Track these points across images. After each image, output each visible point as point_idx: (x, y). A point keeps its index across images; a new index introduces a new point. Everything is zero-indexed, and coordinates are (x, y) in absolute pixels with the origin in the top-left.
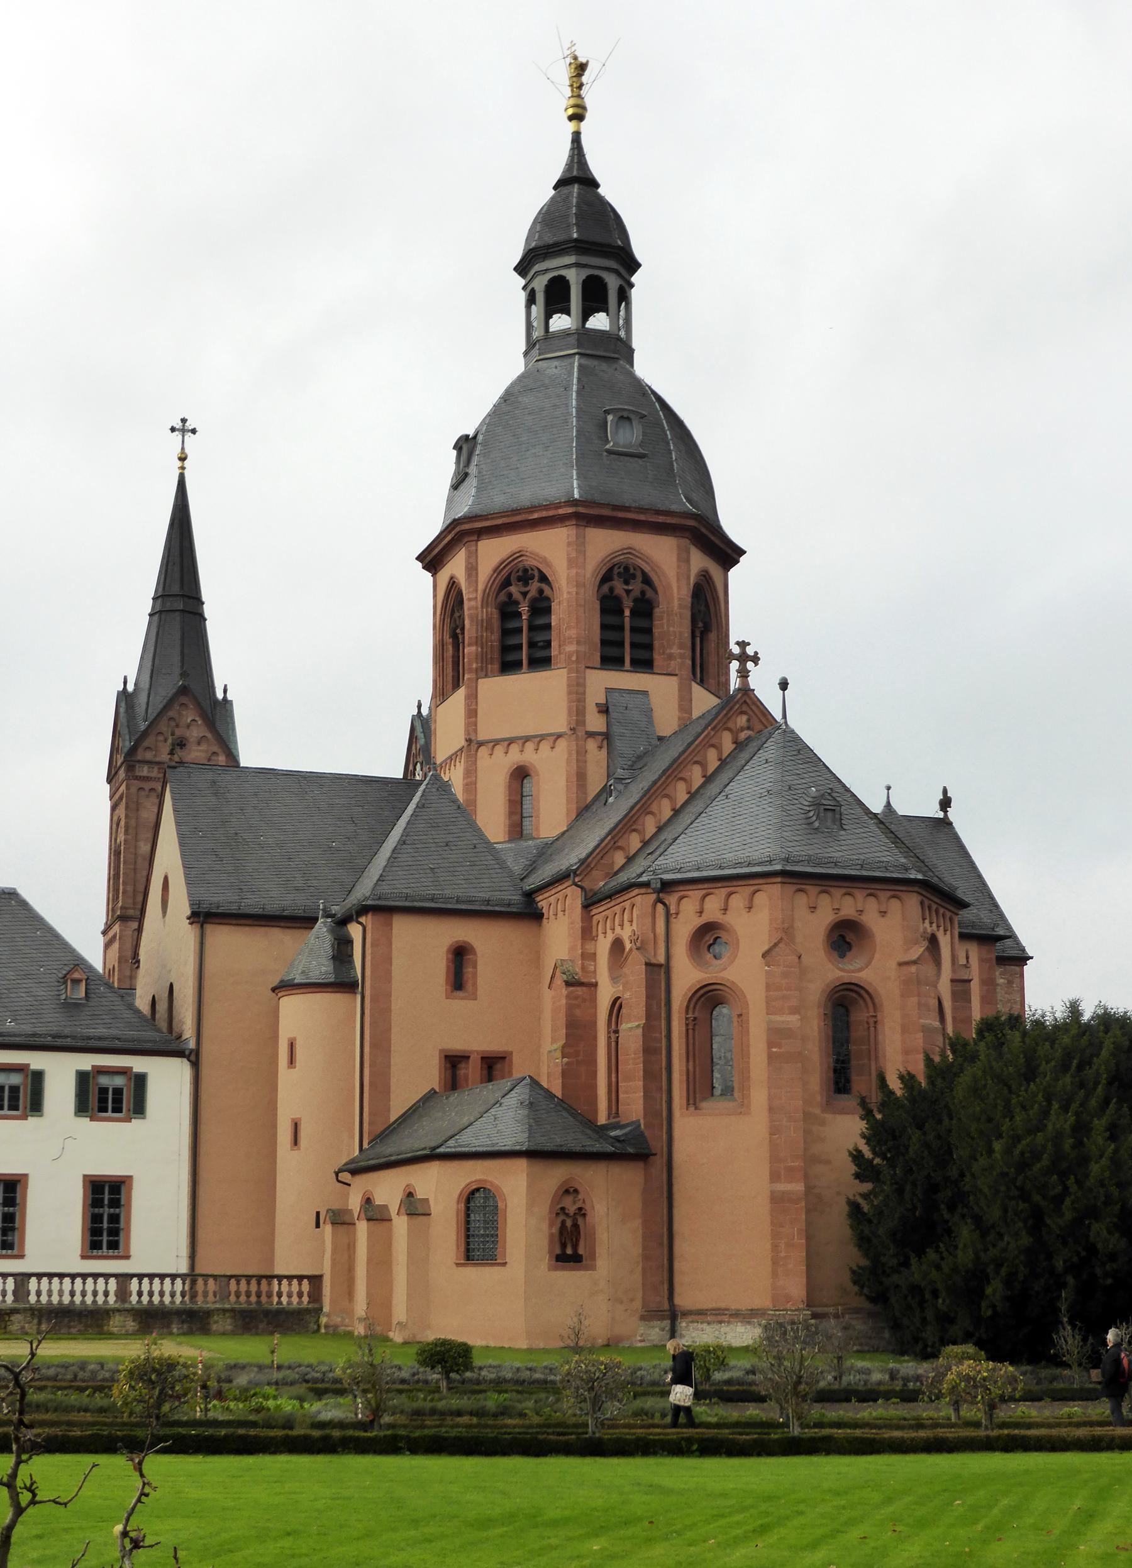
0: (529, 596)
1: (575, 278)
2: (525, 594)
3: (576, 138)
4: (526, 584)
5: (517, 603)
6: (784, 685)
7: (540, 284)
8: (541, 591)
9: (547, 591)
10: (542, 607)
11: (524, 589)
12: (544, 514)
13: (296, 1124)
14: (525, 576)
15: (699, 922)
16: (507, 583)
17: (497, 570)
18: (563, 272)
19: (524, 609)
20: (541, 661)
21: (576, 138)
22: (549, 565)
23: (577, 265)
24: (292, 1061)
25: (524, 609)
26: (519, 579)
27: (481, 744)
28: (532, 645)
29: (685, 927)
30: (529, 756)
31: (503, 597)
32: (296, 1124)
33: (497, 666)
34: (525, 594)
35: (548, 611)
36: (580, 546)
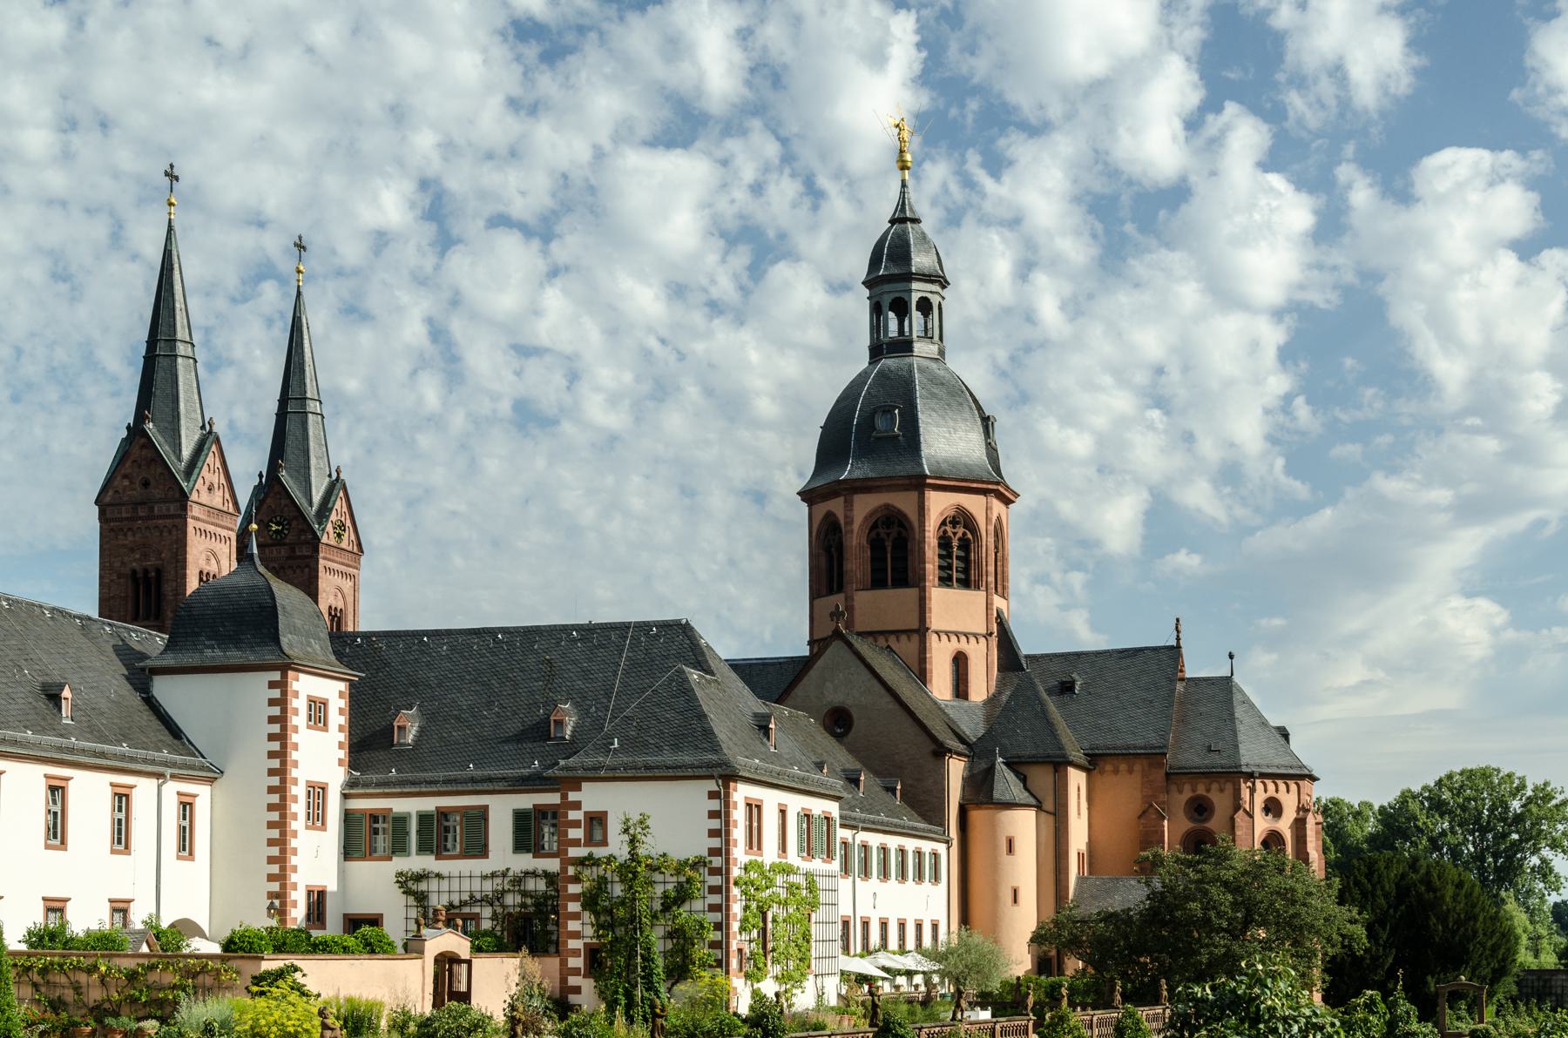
0: (957, 537)
2: (955, 534)
3: (904, 185)
4: (954, 528)
6: (1231, 656)
10: (965, 545)
12: (980, 486)
13: (1015, 890)
14: (954, 522)
16: (944, 523)
17: (941, 514)
18: (929, 296)
19: (955, 543)
20: (966, 583)
24: (1010, 850)
25: (955, 543)
26: (950, 522)
27: (937, 633)
28: (950, 567)
30: (963, 645)
32: (1015, 890)
33: (937, 579)
36: (988, 509)
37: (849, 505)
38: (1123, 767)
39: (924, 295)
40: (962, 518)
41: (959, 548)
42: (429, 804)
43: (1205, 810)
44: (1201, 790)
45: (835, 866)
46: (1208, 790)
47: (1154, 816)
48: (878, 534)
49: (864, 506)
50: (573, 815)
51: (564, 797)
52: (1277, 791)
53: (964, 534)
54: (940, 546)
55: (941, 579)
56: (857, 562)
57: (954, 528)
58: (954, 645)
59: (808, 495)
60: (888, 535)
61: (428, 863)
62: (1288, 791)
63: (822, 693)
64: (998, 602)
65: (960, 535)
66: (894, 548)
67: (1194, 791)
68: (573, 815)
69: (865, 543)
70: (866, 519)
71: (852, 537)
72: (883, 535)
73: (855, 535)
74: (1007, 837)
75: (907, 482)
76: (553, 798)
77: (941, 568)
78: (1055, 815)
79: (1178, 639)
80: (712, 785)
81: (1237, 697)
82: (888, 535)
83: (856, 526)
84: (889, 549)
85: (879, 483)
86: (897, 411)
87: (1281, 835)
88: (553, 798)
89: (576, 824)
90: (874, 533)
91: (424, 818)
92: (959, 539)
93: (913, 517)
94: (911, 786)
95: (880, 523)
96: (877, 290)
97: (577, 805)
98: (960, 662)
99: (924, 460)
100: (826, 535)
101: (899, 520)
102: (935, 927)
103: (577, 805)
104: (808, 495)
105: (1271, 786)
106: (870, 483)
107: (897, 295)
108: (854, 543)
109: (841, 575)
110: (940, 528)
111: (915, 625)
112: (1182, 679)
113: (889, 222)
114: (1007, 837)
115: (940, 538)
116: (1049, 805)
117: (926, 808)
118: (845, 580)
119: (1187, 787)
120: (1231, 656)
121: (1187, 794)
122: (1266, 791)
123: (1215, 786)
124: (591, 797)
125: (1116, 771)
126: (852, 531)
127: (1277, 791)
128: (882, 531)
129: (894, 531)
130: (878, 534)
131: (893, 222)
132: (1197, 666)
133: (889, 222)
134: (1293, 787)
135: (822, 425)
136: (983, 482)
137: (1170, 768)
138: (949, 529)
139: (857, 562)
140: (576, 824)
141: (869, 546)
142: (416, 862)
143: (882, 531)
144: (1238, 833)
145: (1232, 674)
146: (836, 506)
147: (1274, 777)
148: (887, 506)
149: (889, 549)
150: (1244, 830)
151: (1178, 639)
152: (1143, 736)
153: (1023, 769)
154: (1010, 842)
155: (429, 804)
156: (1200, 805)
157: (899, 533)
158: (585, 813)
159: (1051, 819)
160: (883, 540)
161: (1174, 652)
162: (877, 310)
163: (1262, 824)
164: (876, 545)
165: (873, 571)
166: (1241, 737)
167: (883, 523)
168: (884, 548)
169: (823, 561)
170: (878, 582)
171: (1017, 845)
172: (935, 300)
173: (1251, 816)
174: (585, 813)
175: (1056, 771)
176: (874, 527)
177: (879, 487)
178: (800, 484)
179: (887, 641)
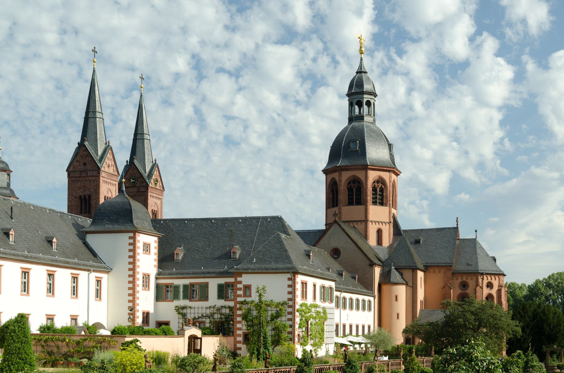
0: (379, 187)
2: (378, 186)
3: (361, 59)
4: (378, 184)
5: (376, 187)
6: (476, 231)
10: (382, 190)
11: (378, 185)
12: (387, 169)
13: (398, 314)
14: (378, 182)
15: (487, 281)
16: (374, 182)
17: (373, 179)
19: (378, 189)
21: (361, 59)
24: (396, 300)
25: (378, 189)
26: (376, 182)
27: (371, 222)
28: (376, 198)
29: (485, 282)
30: (381, 226)
32: (398, 314)
33: (371, 202)
37: (340, 175)
38: (437, 270)
39: (368, 99)
40: (381, 181)
41: (380, 191)
42: (187, 282)
43: (466, 286)
44: (464, 279)
45: (333, 305)
46: (467, 279)
47: (447, 288)
48: (350, 186)
49: (346, 176)
50: (239, 286)
51: (236, 279)
52: (491, 279)
53: (381, 186)
54: (373, 190)
55: (373, 202)
56: (343, 196)
57: (378, 184)
58: (377, 226)
59: (325, 171)
60: (354, 186)
61: (186, 303)
62: (495, 280)
63: (330, 243)
64: (393, 211)
65: (380, 186)
66: (356, 191)
67: (462, 279)
68: (239, 286)
69: (346, 189)
70: (346, 180)
71: (341, 187)
72: (352, 186)
73: (342, 186)
74: (395, 295)
75: (361, 167)
76: (231, 280)
77: (373, 198)
78: (412, 287)
79: (457, 225)
80: (289, 276)
81: (478, 246)
82: (354, 186)
83: (343, 183)
84: (354, 191)
85: (351, 168)
86: (358, 142)
87: (492, 295)
88: (231, 280)
89: (240, 289)
90: (349, 186)
91: (185, 287)
92: (380, 188)
93: (363, 179)
94: (361, 276)
95: (351, 181)
96: (352, 97)
97: (240, 282)
98: (379, 232)
99: (367, 160)
100: (332, 186)
101: (358, 181)
102: (369, 327)
103: (240, 282)
104: (325, 171)
105: (489, 278)
106: (348, 167)
107: (359, 99)
108: (342, 189)
109: (337, 201)
110: (373, 184)
111: (364, 219)
112: (459, 239)
113: (356, 73)
114: (395, 295)
115: (373, 187)
116: (410, 284)
117: (367, 284)
118: (339, 202)
119: (460, 278)
120: (476, 231)
121: (460, 280)
122: (487, 279)
123: (469, 278)
124: (246, 279)
125: (434, 272)
126: (341, 185)
127: (491, 279)
128: (352, 185)
129: (356, 185)
130: (350, 186)
131: (357, 73)
132: (463, 235)
133: (356, 73)
134: (497, 278)
135: (331, 146)
136: (389, 168)
137: (454, 271)
138: (376, 184)
139: (343, 196)
140: (240, 289)
141: (347, 190)
142: (182, 302)
143: (352, 185)
144: (477, 294)
145: (476, 238)
146: (336, 175)
147: (491, 274)
148: (354, 176)
149: (354, 191)
150: (480, 293)
151: (457, 225)
152: (444, 259)
153: (402, 271)
154: (396, 297)
155: (187, 282)
156: (464, 284)
157: (358, 186)
158: (243, 285)
159: (411, 288)
160: (352, 188)
161: (456, 229)
162: (351, 105)
163: (486, 291)
164: (350, 190)
165: (349, 199)
166: (479, 260)
167: (353, 182)
168: (353, 191)
169: (331, 196)
170: (350, 203)
171: (399, 298)
172: (372, 101)
173: (482, 288)
174: (243, 285)
175: (413, 272)
176: (349, 183)
177: (351, 169)
179: (353, 224)
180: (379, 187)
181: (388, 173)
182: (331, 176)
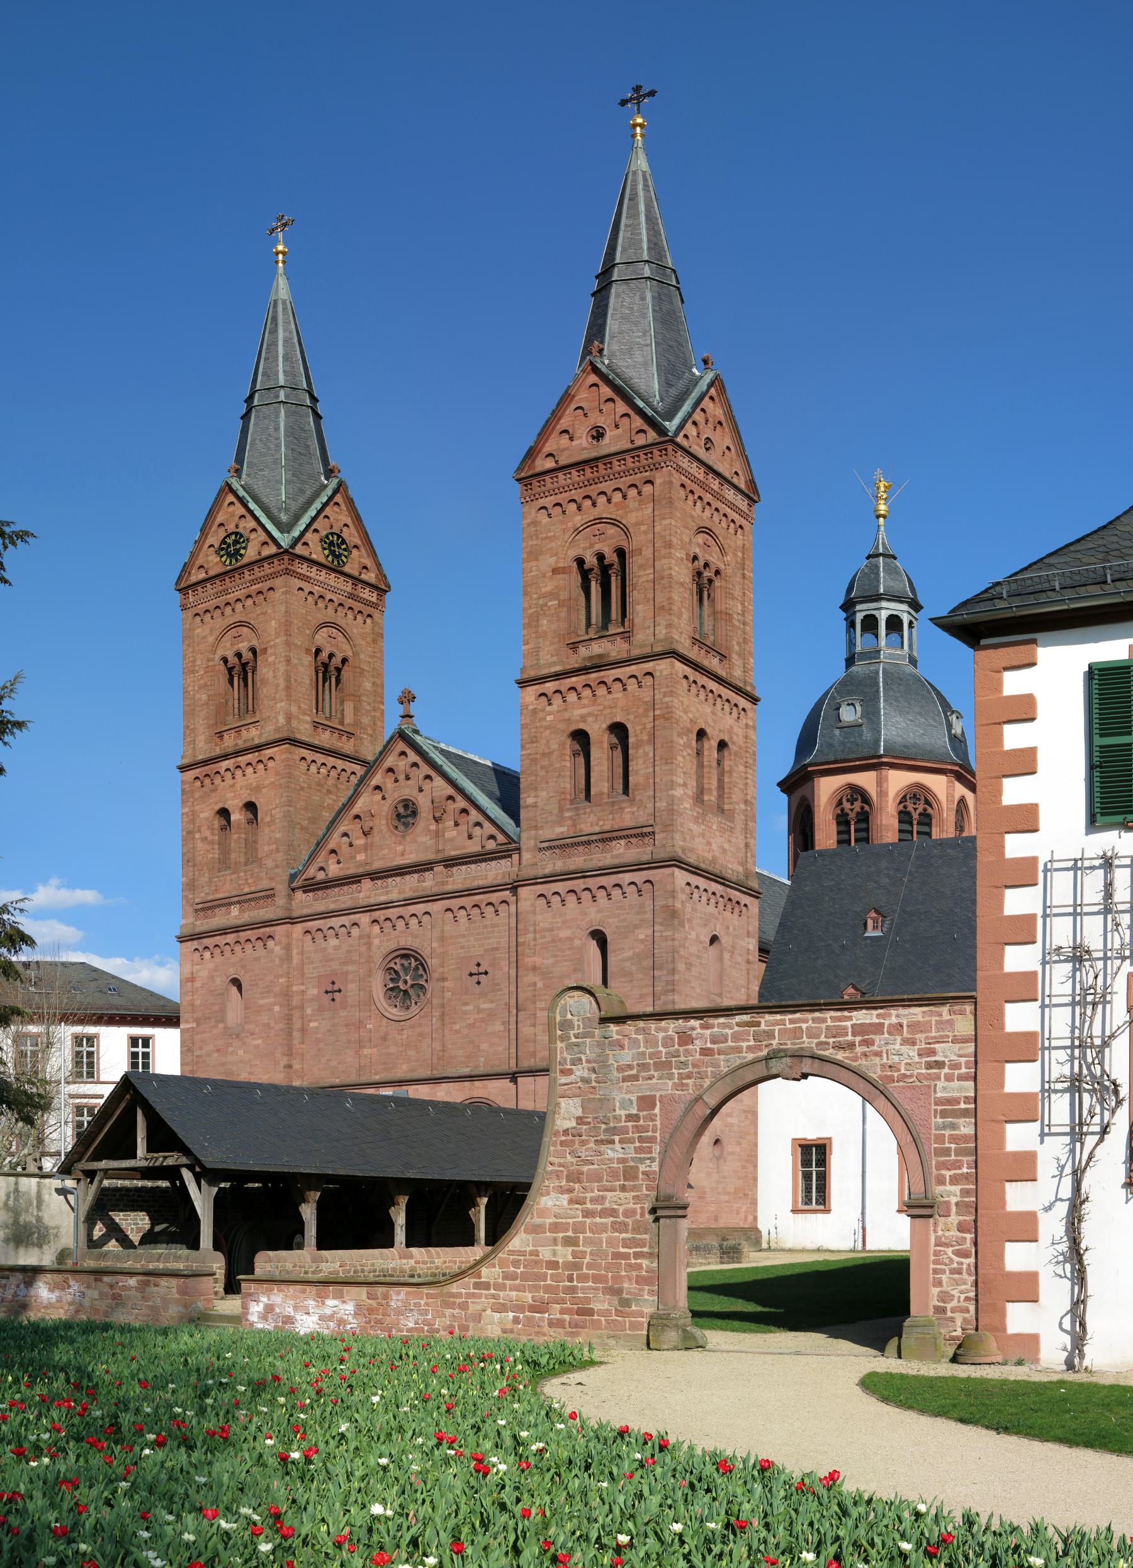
1: (905, 619)
2: (915, 809)
5: (908, 814)
7: (883, 616)
8: (925, 810)
9: (930, 810)
16: (903, 800)
22: (934, 796)
23: (909, 613)
25: (915, 816)
31: (901, 807)
34: (915, 809)
35: (929, 825)
48: (842, 810)
53: (925, 810)
65: (920, 810)
70: (831, 798)
72: (847, 811)
92: (920, 814)
95: (844, 800)
110: (900, 803)
115: (900, 813)
128: (847, 805)
143: (847, 805)
157: (862, 808)
160: (847, 815)
164: (842, 820)
176: (840, 803)
178: (782, 776)
180: (918, 811)
181: (942, 779)
182: (797, 795)
